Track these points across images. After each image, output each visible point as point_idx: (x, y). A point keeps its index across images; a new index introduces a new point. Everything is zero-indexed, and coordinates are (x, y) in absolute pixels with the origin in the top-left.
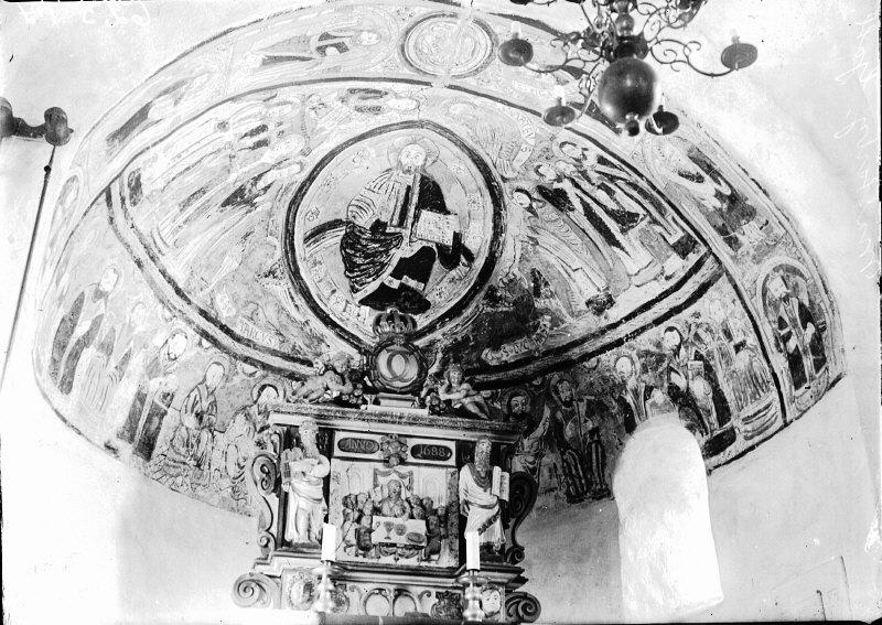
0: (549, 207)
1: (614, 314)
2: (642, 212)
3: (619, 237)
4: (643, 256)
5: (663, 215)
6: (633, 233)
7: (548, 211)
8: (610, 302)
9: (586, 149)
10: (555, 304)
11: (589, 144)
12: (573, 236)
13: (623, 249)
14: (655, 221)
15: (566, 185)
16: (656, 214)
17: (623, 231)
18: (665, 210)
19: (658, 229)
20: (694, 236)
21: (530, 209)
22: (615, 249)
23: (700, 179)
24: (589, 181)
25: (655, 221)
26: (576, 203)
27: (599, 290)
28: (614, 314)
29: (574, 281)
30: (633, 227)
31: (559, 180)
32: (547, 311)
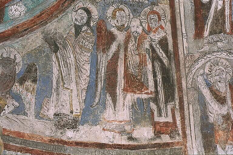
0: (94, 39)
1: (70, 135)
2: (152, 89)
3: (119, 91)
4: (124, 114)
5: (166, 102)
6: (130, 97)
7: (88, 39)
8: (74, 125)
9: (162, 28)
10: (29, 98)
11: (168, 27)
12: (87, 67)
13: (114, 101)
14: (156, 100)
15: (120, 37)
16: (162, 96)
17: (125, 90)
18: (173, 99)
19: (153, 106)
20: (180, 127)
21: (78, 29)
22: (109, 98)
23: (221, 100)
24: (138, 47)
25: (156, 100)
26: (114, 47)
27: (72, 112)
28: (70, 135)
29: (58, 94)
30: (135, 93)
31: (120, 28)
32: (18, 98)
